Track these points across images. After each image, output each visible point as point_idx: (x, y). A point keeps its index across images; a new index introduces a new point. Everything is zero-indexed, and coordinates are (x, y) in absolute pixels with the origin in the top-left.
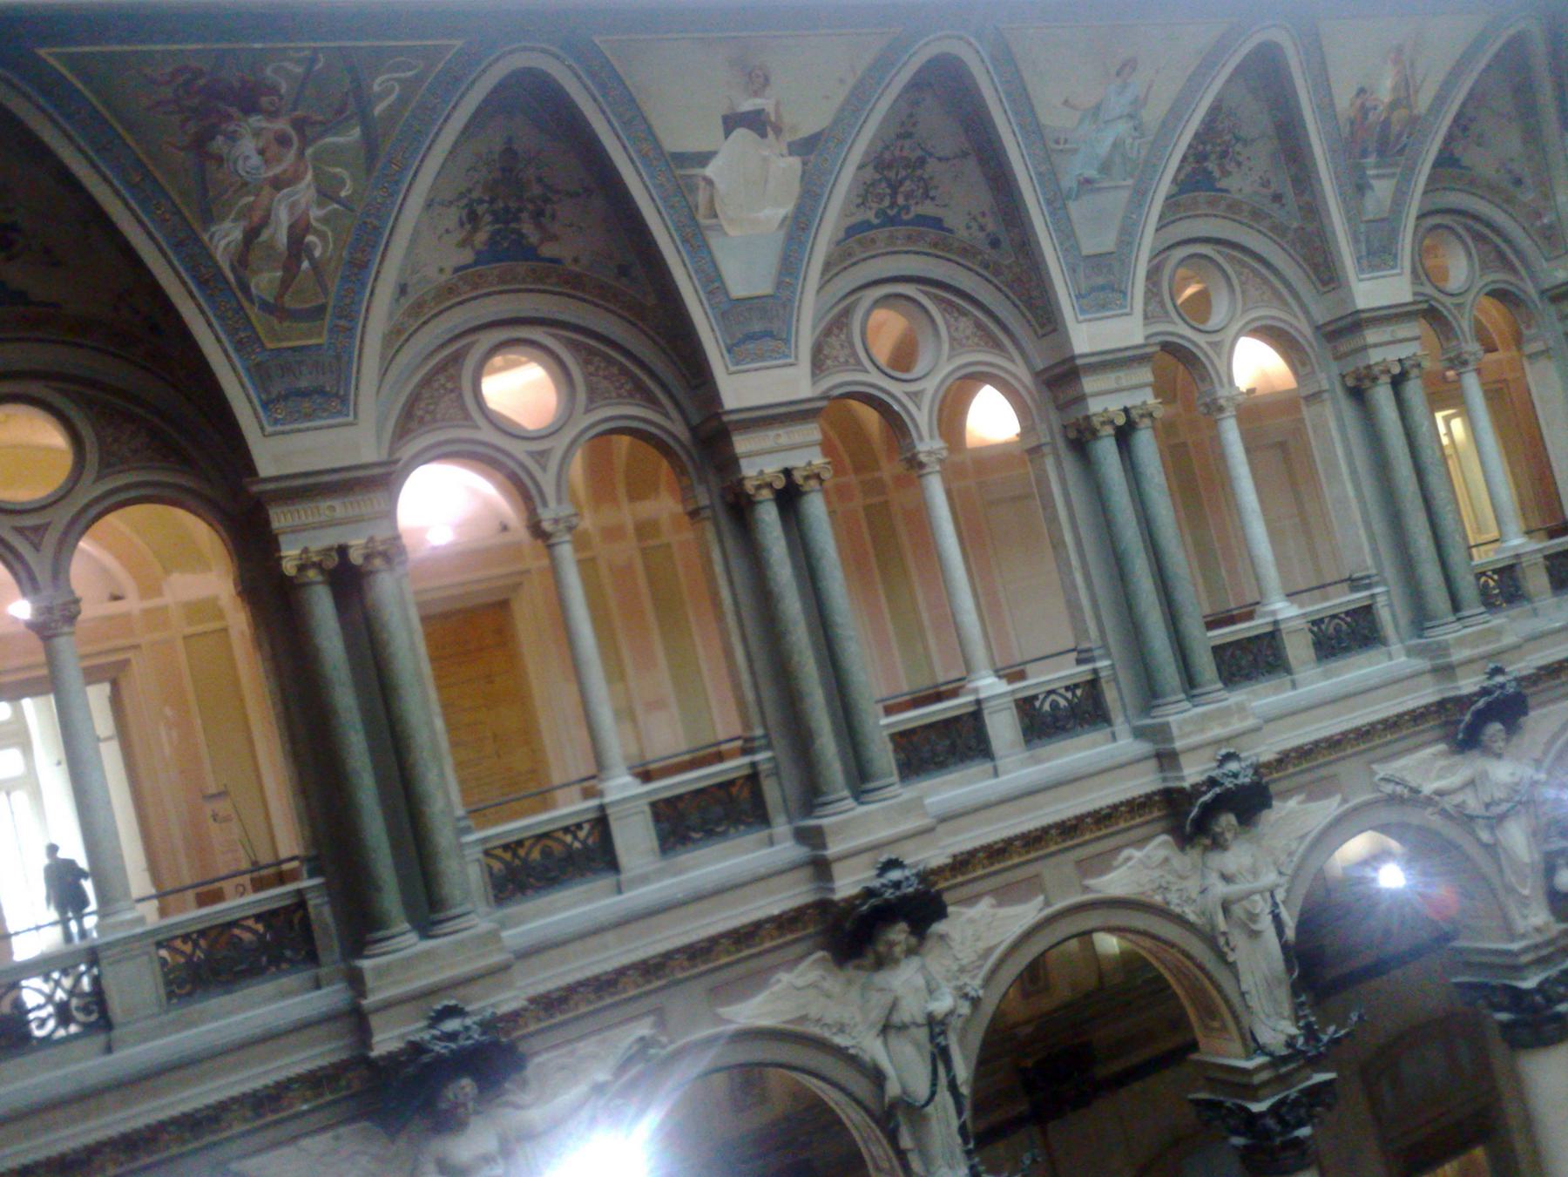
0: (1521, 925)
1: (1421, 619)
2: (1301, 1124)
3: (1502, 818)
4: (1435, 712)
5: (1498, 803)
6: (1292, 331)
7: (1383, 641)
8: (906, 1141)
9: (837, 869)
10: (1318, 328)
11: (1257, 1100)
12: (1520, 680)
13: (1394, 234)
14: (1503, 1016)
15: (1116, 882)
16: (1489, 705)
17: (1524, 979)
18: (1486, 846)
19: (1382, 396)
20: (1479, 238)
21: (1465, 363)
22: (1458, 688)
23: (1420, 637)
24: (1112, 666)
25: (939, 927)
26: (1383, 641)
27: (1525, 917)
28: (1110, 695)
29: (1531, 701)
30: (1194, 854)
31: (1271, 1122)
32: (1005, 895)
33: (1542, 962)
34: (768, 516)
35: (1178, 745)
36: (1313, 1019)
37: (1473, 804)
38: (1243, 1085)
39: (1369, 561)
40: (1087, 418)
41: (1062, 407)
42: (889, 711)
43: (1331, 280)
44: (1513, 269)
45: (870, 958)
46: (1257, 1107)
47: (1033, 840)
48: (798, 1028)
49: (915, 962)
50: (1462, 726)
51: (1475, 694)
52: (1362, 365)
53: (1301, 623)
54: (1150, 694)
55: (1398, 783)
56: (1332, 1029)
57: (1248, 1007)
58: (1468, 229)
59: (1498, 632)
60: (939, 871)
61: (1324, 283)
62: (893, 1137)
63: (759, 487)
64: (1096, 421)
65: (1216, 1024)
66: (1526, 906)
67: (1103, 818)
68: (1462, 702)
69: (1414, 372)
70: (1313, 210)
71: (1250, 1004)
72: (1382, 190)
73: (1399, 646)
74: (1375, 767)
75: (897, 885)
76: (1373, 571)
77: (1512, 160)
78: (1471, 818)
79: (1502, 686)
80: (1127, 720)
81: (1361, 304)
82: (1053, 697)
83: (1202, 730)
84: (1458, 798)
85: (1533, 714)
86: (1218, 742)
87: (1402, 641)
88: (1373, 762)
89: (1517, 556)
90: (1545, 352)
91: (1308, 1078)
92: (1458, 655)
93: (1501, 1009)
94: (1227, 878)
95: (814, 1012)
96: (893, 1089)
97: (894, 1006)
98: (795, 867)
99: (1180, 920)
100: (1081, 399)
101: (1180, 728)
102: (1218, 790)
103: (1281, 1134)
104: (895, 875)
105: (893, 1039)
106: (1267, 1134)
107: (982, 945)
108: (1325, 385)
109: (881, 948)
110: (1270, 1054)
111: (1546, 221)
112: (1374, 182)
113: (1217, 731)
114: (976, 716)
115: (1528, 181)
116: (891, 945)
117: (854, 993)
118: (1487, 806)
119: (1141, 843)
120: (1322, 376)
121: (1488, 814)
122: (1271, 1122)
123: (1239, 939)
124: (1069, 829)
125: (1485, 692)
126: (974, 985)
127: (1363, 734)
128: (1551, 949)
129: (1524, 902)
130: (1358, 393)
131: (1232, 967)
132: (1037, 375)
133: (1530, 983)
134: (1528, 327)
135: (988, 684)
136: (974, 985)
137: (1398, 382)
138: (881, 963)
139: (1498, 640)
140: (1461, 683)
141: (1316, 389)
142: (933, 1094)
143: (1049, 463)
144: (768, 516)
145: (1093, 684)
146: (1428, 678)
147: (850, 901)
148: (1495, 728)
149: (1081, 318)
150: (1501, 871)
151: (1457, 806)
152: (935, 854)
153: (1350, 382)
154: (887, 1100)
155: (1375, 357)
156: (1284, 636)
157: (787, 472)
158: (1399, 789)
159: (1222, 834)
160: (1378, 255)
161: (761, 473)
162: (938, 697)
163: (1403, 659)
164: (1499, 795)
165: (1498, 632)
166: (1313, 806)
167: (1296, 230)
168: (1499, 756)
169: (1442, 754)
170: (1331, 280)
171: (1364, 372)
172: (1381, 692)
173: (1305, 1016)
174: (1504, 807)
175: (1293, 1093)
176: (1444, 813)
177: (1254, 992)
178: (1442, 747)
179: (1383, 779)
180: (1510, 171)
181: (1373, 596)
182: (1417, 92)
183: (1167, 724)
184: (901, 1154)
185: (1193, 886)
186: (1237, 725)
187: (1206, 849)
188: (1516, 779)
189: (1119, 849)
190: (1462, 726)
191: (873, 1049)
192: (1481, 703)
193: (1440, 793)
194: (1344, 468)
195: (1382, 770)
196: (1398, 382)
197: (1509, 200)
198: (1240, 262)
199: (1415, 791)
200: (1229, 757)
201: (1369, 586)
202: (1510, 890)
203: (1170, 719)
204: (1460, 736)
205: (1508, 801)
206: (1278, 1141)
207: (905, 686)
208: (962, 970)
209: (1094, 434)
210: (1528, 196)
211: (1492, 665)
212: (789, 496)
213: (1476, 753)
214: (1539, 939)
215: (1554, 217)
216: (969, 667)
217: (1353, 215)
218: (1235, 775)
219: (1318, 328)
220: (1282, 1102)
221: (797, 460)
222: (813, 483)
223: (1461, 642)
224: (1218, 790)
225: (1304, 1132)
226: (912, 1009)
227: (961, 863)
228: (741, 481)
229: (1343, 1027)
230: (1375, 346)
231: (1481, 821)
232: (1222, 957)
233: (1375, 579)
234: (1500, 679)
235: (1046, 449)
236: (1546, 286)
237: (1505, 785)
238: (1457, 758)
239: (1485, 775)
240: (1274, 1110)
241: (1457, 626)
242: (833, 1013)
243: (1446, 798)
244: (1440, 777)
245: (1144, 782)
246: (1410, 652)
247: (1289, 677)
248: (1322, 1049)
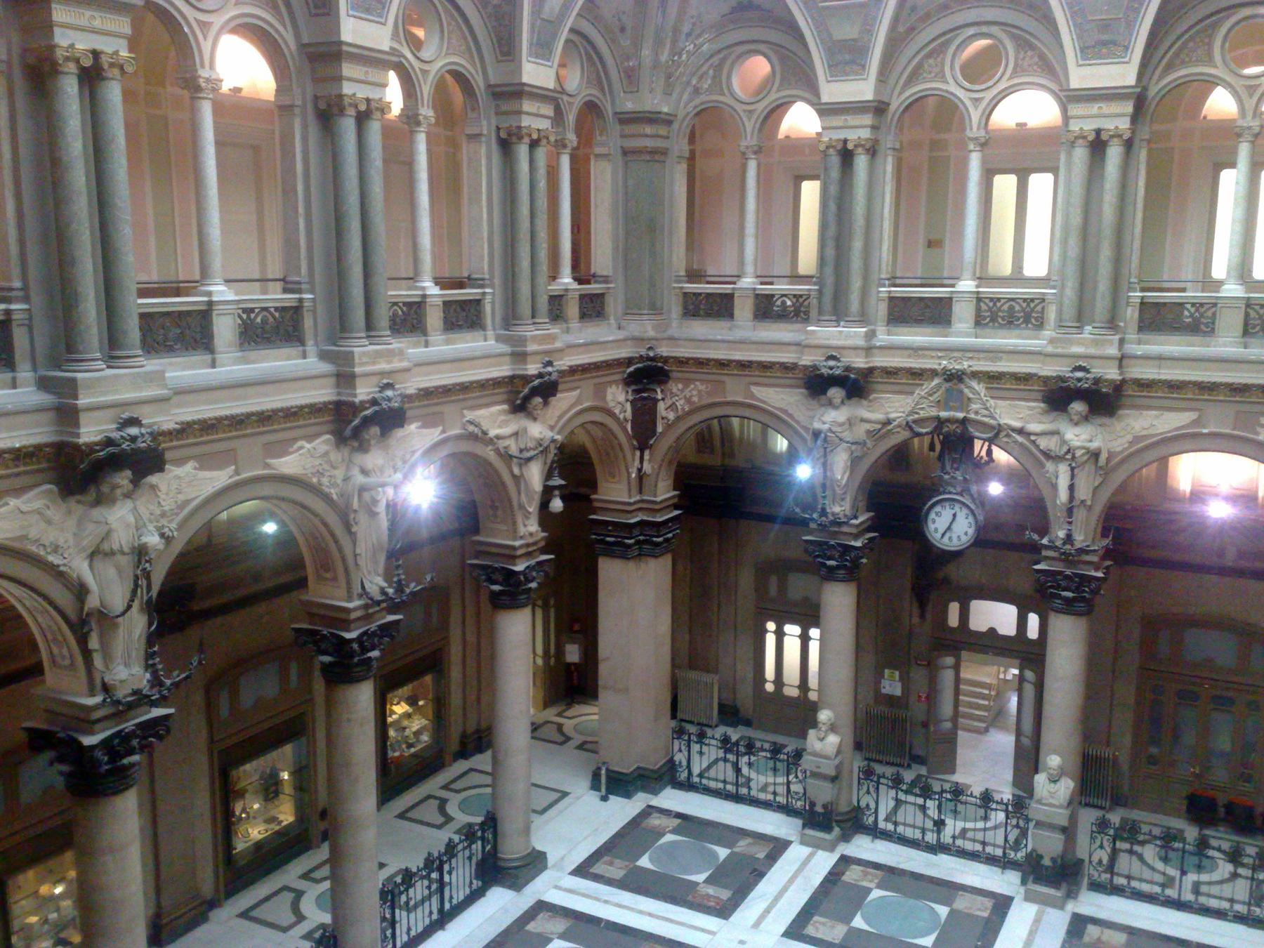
0: (522, 530)
1: (510, 317)
2: (373, 648)
3: (529, 460)
4: (507, 383)
5: (527, 450)
6: (473, 82)
7: (483, 328)
8: (94, 643)
9: (83, 418)
11: (348, 630)
12: (560, 372)
13: (554, 36)
14: (496, 588)
15: (289, 464)
16: (541, 384)
17: (515, 565)
18: (514, 476)
19: (522, 150)
20: (590, 58)
21: (565, 146)
22: (526, 369)
23: (506, 330)
24: (314, 300)
25: (154, 479)
26: (483, 328)
27: (525, 526)
28: (308, 322)
29: (560, 387)
30: (346, 451)
31: (355, 646)
32: (206, 462)
33: (529, 555)
34: (70, 87)
35: (357, 370)
36: (403, 577)
37: (514, 450)
38: (340, 619)
39: (486, 267)
40: (341, 96)
41: (316, 80)
42: (143, 293)
43: (508, 53)
44: (604, 94)
45: (92, 495)
46: (348, 636)
47: (237, 422)
48: (16, 545)
49: (129, 504)
51: (533, 376)
52: (515, 124)
53: (439, 301)
54: (340, 327)
55: (476, 426)
56: (413, 585)
57: (357, 564)
58: (587, 53)
59: (552, 338)
60: (170, 434)
62: (83, 641)
63: (67, 59)
64: (347, 101)
65: (328, 575)
66: (527, 518)
67: (291, 414)
68: (526, 379)
69: (544, 142)
71: (359, 563)
73: (492, 332)
74: (465, 412)
75: (133, 439)
76: (487, 276)
77: (624, 13)
78: (511, 457)
79: (550, 374)
80: (316, 344)
81: (526, 79)
82: (784, 298)
83: (374, 363)
84: (507, 442)
85: (559, 395)
86: (383, 374)
87: (494, 329)
88: (466, 408)
89: (567, 290)
90: (605, 156)
91: (384, 618)
92: (532, 347)
93: (495, 583)
94: (364, 472)
95: (33, 533)
96: (93, 602)
97: (108, 535)
98: (40, 410)
99: (327, 498)
100: (339, 79)
101: (360, 359)
102: (376, 408)
103: (359, 655)
104: (134, 431)
105: (99, 564)
106: (352, 654)
107: (181, 497)
108: (485, 132)
109: (105, 489)
110: (371, 599)
113: (383, 366)
114: (205, 315)
116: (115, 487)
117: (71, 523)
118: (521, 451)
119: (311, 438)
120: (484, 123)
121: (521, 456)
122: (355, 646)
123: (363, 518)
124: (264, 418)
125: (540, 375)
126: (172, 526)
127: (464, 388)
128: (535, 548)
129: (527, 515)
130: (506, 145)
131: (353, 536)
132: (302, 46)
133: (519, 567)
134: (601, 135)
135: (220, 291)
136: (172, 526)
137: (534, 144)
138: (98, 502)
139: (553, 343)
140: (529, 366)
141: (478, 132)
142: (129, 607)
143: (297, 123)
144: (70, 87)
145: (297, 310)
146: (507, 359)
147: (91, 447)
148: (538, 400)
149: (351, 12)
150: (519, 493)
151: (505, 448)
152: (167, 420)
153: (503, 135)
154: (86, 609)
155: (526, 122)
156: (428, 308)
157: (96, 54)
158: (476, 430)
159: (369, 440)
160: (542, 49)
161: (72, 46)
162: (177, 292)
163: (493, 342)
164: (531, 445)
165: (552, 338)
166: (425, 431)
167: (495, 6)
168: (535, 419)
169: (501, 412)
171: (515, 131)
172: (480, 361)
173: (399, 575)
174: (532, 453)
175: (373, 627)
176: (497, 451)
177: (363, 555)
178: (505, 407)
179: (469, 421)
180: (619, 20)
181: (484, 293)
183: (352, 352)
184: (87, 654)
185: (339, 474)
186: (397, 364)
187: (354, 450)
188: (542, 436)
189: (295, 440)
190: (522, 395)
191: (81, 568)
192: (536, 382)
193: (498, 437)
194: (484, 197)
195: (470, 415)
196: (534, 144)
197: (613, 41)
198: (452, 16)
199: (485, 433)
200: (389, 386)
201: (482, 286)
202: (522, 507)
203: (355, 349)
204: (519, 402)
205: (534, 449)
206: (356, 660)
207: (153, 275)
208: (163, 515)
209: (342, 111)
210: (625, 42)
211: (547, 359)
212: (92, 75)
213: (522, 415)
214: (531, 540)
215: (637, 63)
216: (205, 272)
218: (389, 400)
219: (489, 86)
220: (365, 633)
221: (107, 46)
222: (116, 72)
223: (534, 338)
224: (376, 408)
225: (375, 654)
226: (122, 538)
227: (185, 430)
228: (52, 47)
229: (420, 584)
230: (528, 114)
231: (515, 460)
232: (348, 526)
233: (487, 282)
234: (550, 369)
235: (297, 111)
236: (618, 110)
237: (536, 439)
238: (512, 416)
239: (525, 430)
240: (359, 639)
241: (532, 327)
242: (51, 536)
243: (500, 441)
244: (500, 427)
245: (323, 393)
246: (499, 339)
247: (424, 338)
248: (404, 598)
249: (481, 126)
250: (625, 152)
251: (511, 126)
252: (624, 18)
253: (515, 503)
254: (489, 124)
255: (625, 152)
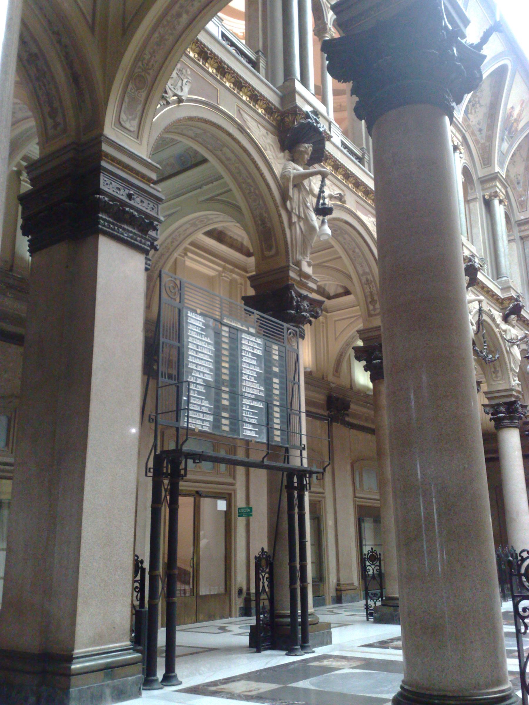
10: (479, 178)
43: (488, 164)
50: (509, 308)
61: (484, 165)
70: (490, 138)
72: (505, 145)
77: (519, 175)
111: (522, 199)
112: (505, 141)
115: (521, 184)
130: (488, 204)
167: (482, 144)
170: (488, 164)
180: (517, 178)
182: (521, 121)
197: (514, 188)
210: (520, 189)
215: (525, 199)
217: (500, 146)
249: (476, 194)
250: (522, 238)
251: (491, 192)
252: (519, 177)
253: (508, 366)
254: (480, 194)
255: (522, 238)
